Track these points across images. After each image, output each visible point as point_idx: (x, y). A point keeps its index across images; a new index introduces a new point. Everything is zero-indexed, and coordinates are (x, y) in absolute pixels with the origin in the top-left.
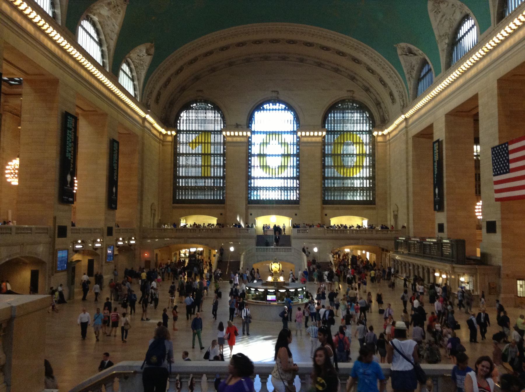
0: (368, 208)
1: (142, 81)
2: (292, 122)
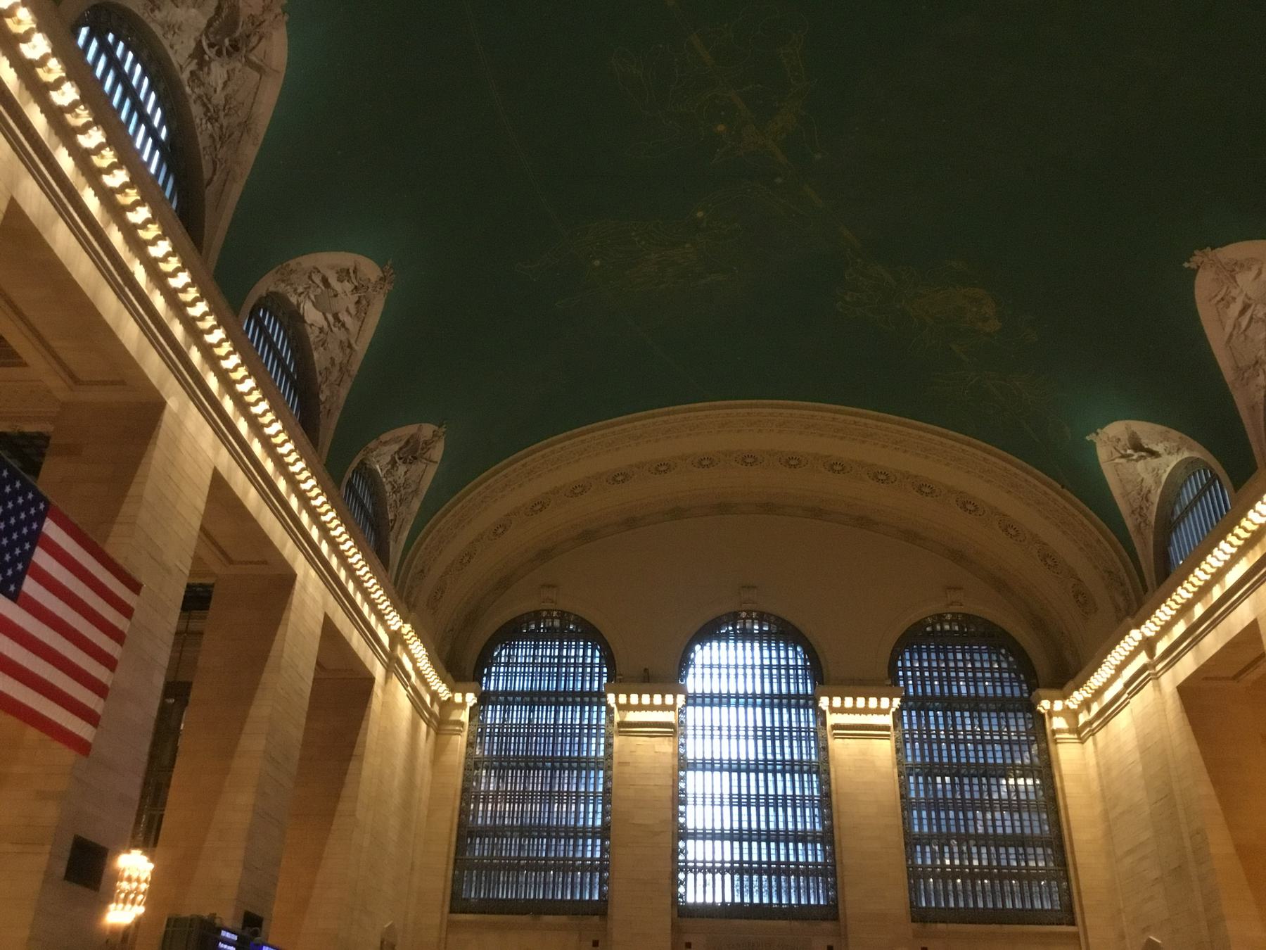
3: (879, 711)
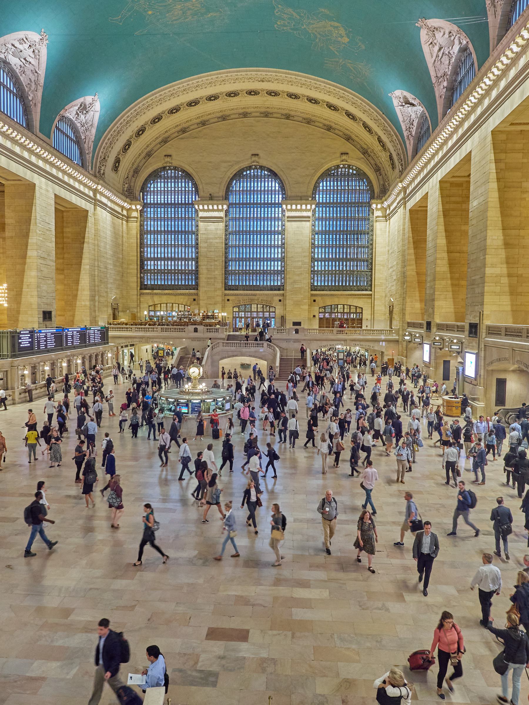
3: (306, 210)
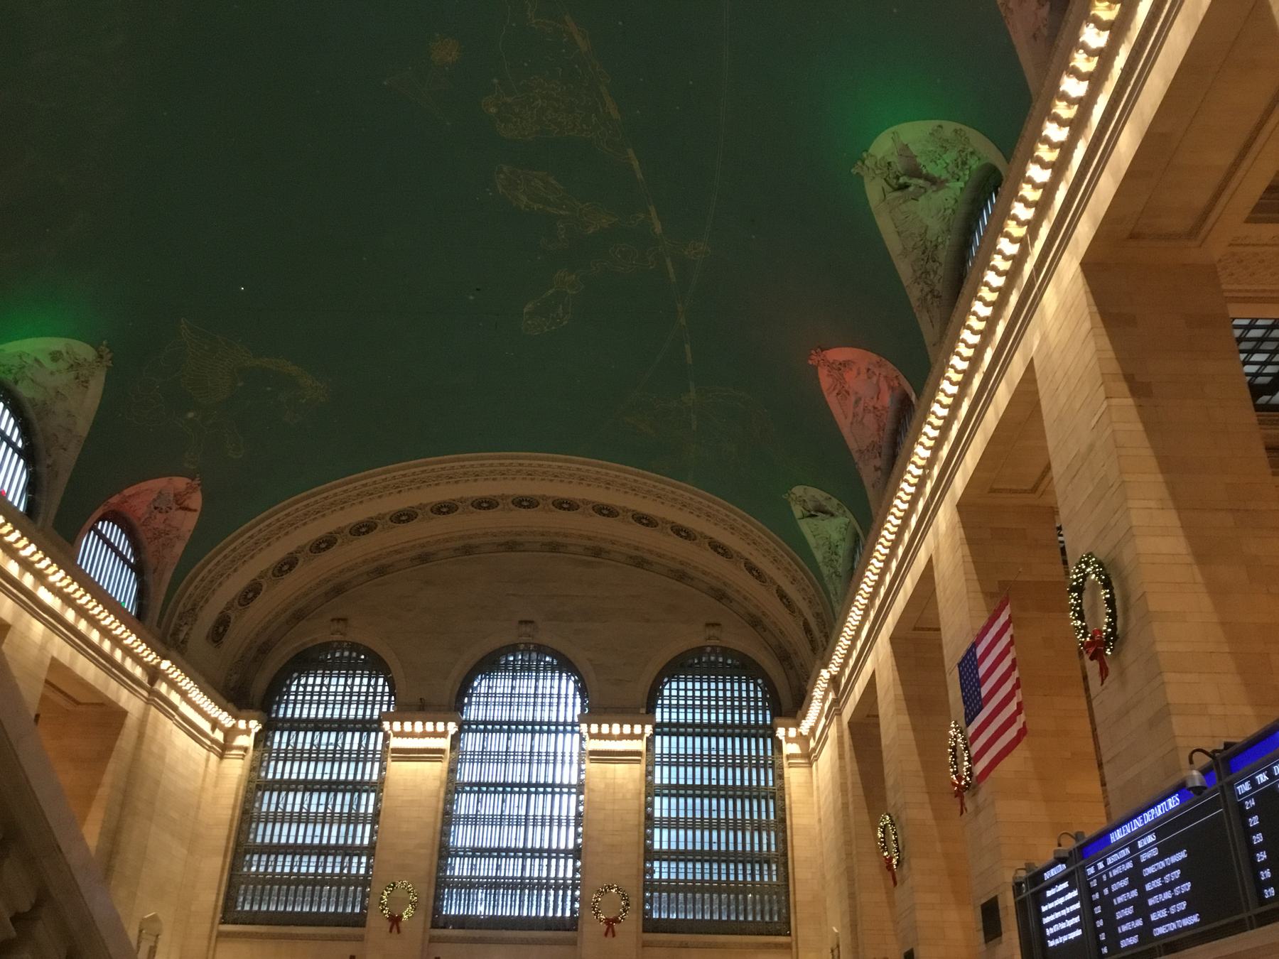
0: (767, 946)
1: (168, 576)
2: (570, 701)
3: (632, 736)
